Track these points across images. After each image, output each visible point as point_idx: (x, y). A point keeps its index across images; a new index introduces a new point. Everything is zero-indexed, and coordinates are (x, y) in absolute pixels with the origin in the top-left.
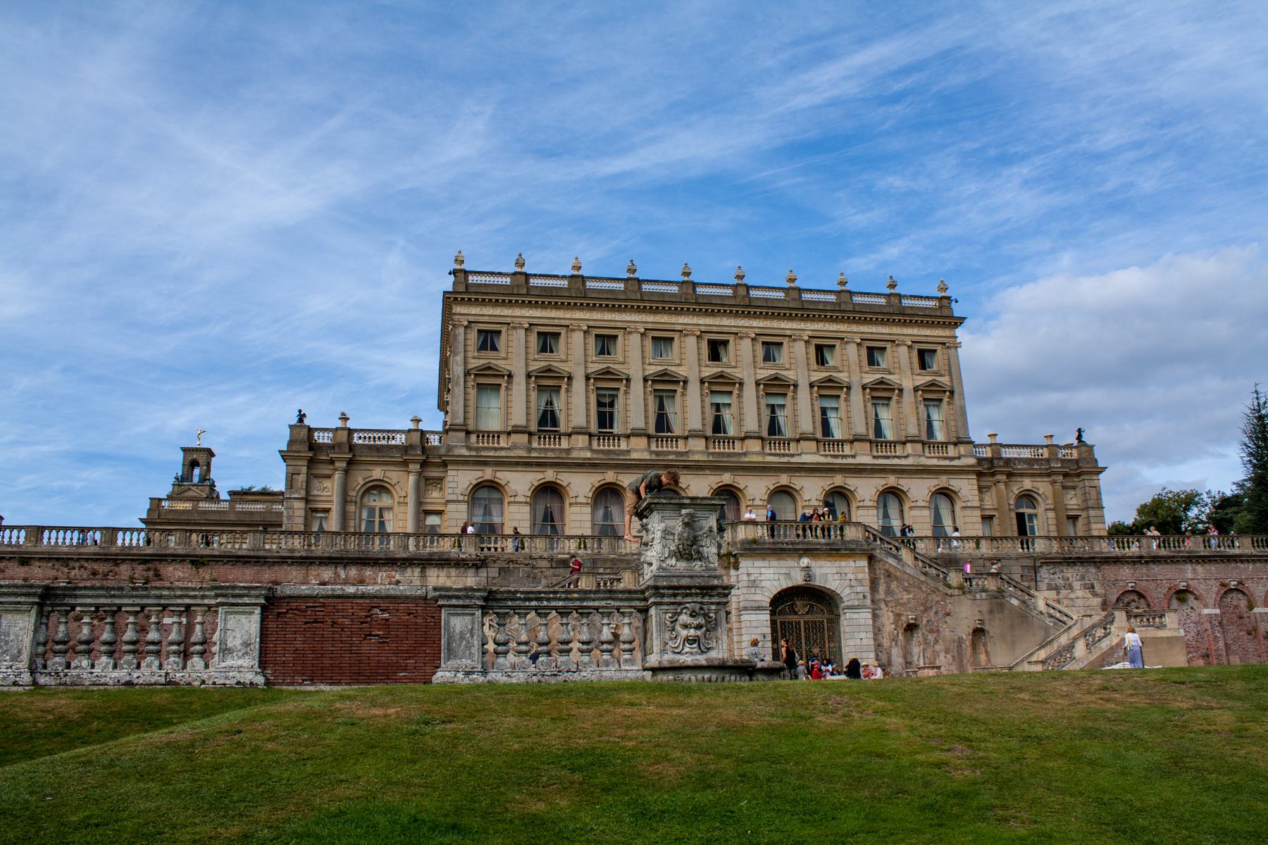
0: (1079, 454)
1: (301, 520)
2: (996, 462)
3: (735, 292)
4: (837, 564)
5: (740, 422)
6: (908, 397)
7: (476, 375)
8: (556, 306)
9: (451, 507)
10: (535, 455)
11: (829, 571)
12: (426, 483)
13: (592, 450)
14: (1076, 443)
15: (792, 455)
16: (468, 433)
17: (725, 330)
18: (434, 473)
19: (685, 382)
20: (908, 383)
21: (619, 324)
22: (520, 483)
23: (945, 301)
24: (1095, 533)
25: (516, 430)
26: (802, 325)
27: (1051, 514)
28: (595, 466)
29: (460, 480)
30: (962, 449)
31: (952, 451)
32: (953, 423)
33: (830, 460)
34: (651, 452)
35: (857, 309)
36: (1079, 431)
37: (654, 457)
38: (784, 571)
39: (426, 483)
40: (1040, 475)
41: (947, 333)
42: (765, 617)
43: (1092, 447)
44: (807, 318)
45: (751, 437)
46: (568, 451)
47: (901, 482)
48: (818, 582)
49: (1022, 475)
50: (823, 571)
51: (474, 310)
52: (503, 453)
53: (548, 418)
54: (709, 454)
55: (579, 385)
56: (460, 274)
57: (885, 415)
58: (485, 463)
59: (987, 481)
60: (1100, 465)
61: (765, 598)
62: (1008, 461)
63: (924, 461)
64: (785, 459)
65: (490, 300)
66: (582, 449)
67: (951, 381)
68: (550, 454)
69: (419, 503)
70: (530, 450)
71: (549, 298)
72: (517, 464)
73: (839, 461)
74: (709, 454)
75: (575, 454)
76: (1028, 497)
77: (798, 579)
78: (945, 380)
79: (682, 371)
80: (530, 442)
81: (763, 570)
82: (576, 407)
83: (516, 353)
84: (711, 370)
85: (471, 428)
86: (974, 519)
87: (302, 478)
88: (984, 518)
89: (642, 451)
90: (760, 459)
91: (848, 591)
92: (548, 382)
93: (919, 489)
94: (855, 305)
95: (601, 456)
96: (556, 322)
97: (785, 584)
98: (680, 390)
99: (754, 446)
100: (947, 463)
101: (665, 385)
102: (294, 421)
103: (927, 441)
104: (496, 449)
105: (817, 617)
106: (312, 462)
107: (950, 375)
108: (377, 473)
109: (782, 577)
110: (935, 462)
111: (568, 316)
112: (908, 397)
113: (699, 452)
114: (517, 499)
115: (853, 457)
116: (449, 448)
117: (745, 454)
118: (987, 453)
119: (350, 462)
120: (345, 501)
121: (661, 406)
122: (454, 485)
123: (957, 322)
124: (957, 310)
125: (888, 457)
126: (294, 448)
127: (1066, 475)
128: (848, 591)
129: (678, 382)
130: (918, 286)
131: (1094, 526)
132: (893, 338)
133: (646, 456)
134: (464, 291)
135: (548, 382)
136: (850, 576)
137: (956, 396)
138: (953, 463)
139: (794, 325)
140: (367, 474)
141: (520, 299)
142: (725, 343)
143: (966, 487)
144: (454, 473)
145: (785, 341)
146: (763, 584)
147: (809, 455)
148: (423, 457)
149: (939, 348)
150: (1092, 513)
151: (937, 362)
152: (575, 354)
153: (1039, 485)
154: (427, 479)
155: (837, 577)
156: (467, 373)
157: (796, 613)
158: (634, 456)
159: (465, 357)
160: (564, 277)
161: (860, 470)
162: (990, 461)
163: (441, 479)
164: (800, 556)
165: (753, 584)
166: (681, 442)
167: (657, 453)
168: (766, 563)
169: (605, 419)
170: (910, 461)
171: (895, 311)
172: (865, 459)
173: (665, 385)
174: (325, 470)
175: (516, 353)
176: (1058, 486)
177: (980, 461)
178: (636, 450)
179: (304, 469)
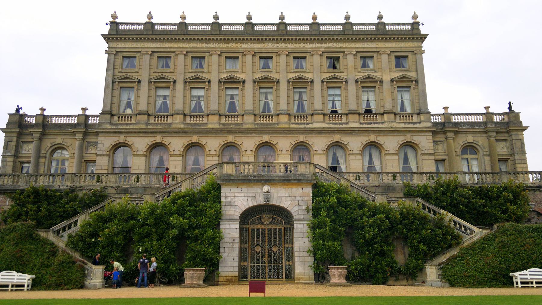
0: (509, 118)
1: (11, 168)
2: (447, 125)
3: (278, 28)
4: (290, 190)
5: (277, 104)
6: (386, 86)
7: (119, 82)
8: (168, 40)
9: (98, 159)
10: (151, 127)
11: (283, 195)
12: (85, 145)
13: (184, 123)
14: (508, 111)
15: (307, 124)
17: (270, 50)
19: (244, 82)
20: (386, 78)
21: (206, 50)
23: (415, 25)
24: (519, 170)
25: (141, 113)
26: (319, 45)
27: (487, 158)
28: (186, 132)
29: (106, 142)
30: (422, 117)
31: (415, 118)
32: (417, 101)
34: (220, 124)
35: (356, 33)
36: (510, 103)
37: (221, 126)
38: (251, 195)
39: (85, 145)
40: (479, 132)
41: (416, 44)
42: (236, 226)
43: (518, 114)
44: (322, 41)
45: (282, 114)
46: (170, 124)
47: (379, 138)
48: (274, 202)
49: (466, 133)
50: (280, 195)
51: (121, 45)
52: (131, 126)
54: (255, 124)
56: (114, 25)
58: (120, 133)
59: (440, 137)
60: (524, 125)
62: (457, 124)
63: (395, 125)
64: (303, 126)
65: (129, 39)
66: (179, 123)
67: (417, 75)
68: (159, 126)
69: (81, 156)
72: (139, 132)
73: (338, 126)
74: (255, 124)
75: (174, 126)
77: (260, 200)
78: (413, 75)
79: (242, 76)
80: (148, 119)
81: (237, 194)
85: (114, 113)
86: (430, 162)
87: (13, 144)
88: (436, 161)
89: (214, 123)
90: (287, 126)
91: (296, 208)
93: (391, 143)
94: (353, 31)
95: (190, 127)
96: (168, 50)
98: (241, 87)
99: (284, 119)
100: (411, 126)
102: (13, 111)
103: (402, 114)
104: (127, 124)
107: (417, 71)
108: (59, 140)
109: (249, 199)
110: (403, 125)
111: (176, 46)
112: (386, 86)
113: (250, 123)
114: (138, 153)
115: (347, 123)
117: (277, 124)
118: (439, 119)
119: (43, 134)
120: (38, 155)
122: (101, 146)
123: (423, 38)
124: (423, 30)
125: (370, 123)
126: (10, 127)
127: (498, 132)
128: (296, 208)
129: (239, 82)
130: (397, 16)
131: (518, 166)
132: (378, 50)
133: (217, 126)
134: (116, 34)
136: (298, 198)
137: (420, 82)
138: (416, 126)
139: (314, 45)
140: (52, 141)
141: (146, 37)
143: (425, 142)
144: (102, 138)
145: (308, 56)
146: (236, 204)
149: (410, 55)
150: (517, 157)
151: (409, 63)
153: (479, 139)
154: (88, 143)
155: (289, 199)
157: (262, 223)
158: (210, 126)
159: (114, 72)
160: (175, 24)
161: (351, 132)
162: (443, 124)
163: (96, 143)
164: (263, 184)
166: (240, 118)
167: (224, 124)
168: (239, 190)
170: (385, 125)
171: (381, 32)
172: (354, 124)
174: (29, 139)
175: (144, 69)
176: (492, 140)
177: (436, 124)
178: (211, 123)
179: (15, 139)
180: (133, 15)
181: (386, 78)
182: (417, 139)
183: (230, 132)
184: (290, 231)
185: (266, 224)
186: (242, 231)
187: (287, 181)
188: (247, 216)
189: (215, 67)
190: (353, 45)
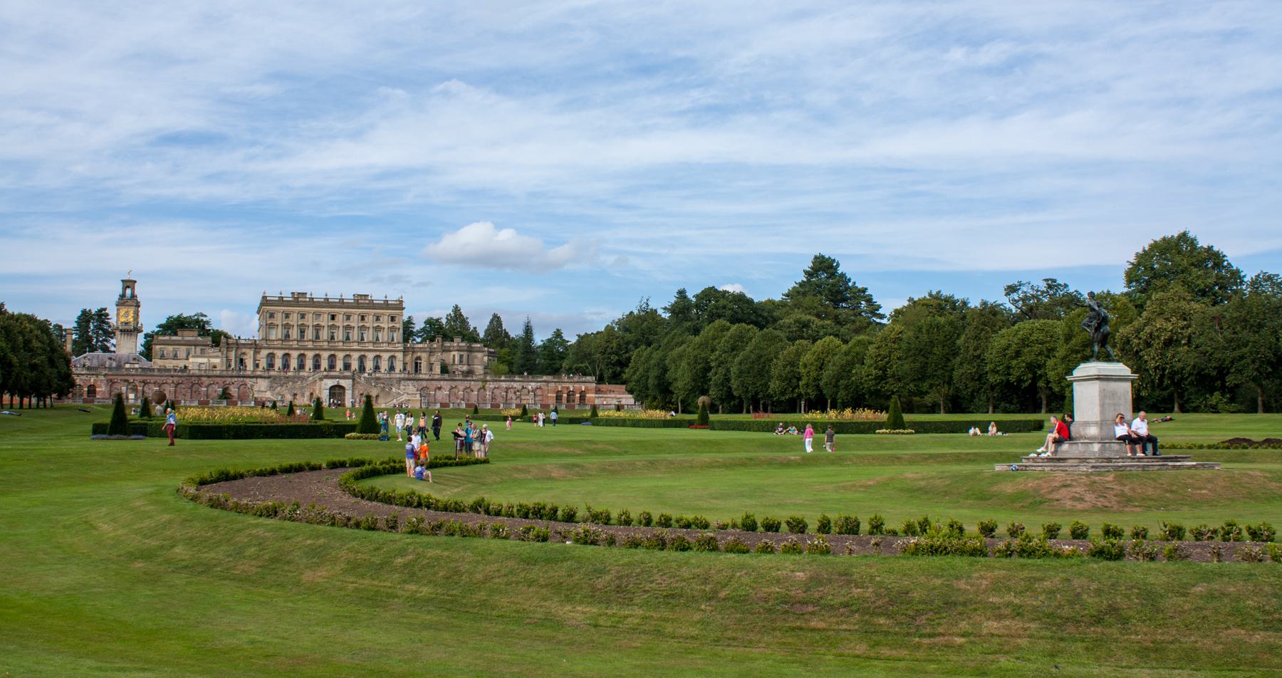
12: (256, 353)
22: (279, 353)
29: (264, 353)
39: (256, 353)
53: (287, 336)
56: (264, 298)
57: (380, 335)
71: (288, 304)
76: (419, 358)
82: (294, 333)
92: (287, 327)
101: (318, 328)
130: (393, 298)
135: (287, 327)
147: (355, 346)
148: (256, 347)
152: (294, 320)
169: (302, 336)
171: (386, 305)
173: (318, 328)
175: (279, 319)
180: (273, 294)
187: (345, 378)
188: (332, 388)
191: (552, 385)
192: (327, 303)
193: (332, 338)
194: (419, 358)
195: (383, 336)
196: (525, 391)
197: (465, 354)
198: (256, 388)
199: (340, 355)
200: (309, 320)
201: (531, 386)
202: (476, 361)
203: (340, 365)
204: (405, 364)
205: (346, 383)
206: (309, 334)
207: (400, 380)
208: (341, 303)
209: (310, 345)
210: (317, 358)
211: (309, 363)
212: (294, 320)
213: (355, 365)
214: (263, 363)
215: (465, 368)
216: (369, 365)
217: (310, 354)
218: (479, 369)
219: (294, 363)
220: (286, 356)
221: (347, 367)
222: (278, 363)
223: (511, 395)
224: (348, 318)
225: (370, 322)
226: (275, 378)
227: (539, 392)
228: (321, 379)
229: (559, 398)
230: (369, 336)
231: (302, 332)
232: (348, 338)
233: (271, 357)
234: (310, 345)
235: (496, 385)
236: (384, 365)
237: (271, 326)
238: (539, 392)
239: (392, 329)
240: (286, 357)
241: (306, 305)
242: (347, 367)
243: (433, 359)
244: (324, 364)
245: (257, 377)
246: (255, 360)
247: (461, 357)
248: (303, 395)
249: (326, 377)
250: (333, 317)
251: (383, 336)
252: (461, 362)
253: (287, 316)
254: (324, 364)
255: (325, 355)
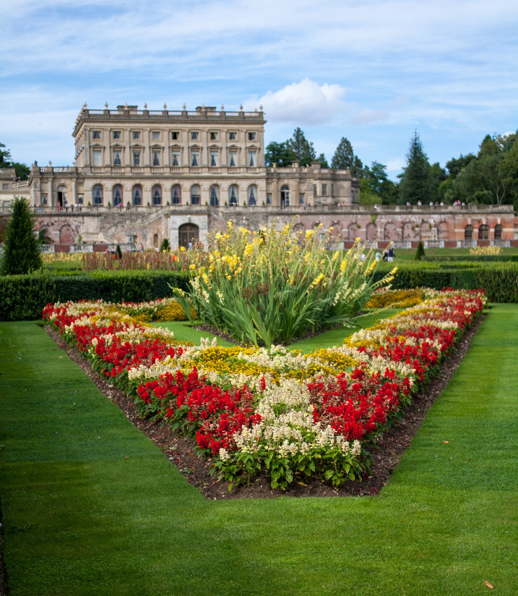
5: (182, 162)
6: (243, 151)
9: (86, 193)
12: (79, 184)
16: (91, 168)
18: (81, 181)
20: (243, 146)
22: (108, 184)
25: (107, 167)
29: (89, 184)
33: (212, 175)
34: (151, 173)
39: (79, 184)
40: (291, 178)
41: (260, 126)
46: (124, 173)
49: (284, 179)
51: (92, 124)
53: (117, 162)
55: (127, 150)
57: (235, 157)
61: (177, 226)
70: (112, 173)
71: (117, 119)
75: (126, 174)
76: (286, 187)
77: (187, 221)
78: (257, 145)
79: (162, 144)
82: (126, 158)
83: (105, 140)
84: (173, 143)
85: (92, 165)
97: (183, 222)
105: (193, 231)
106: (41, 179)
116: (85, 173)
121: (156, 156)
123: (264, 122)
129: (160, 148)
142: (178, 133)
147: (205, 173)
148: (77, 176)
156: (90, 147)
158: (146, 174)
165: (174, 223)
169: (137, 161)
170: (241, 175)
171: (242, 118)
172: (225, 174)
175: (105, 140)
179: (39, 181)
181: (243, 146)
182: (257, 182)
183: (157, 178)
184: (197, 233)
185: (188, 231)
186: (180, 233)
187: (197, 213)
189: (146, 139)
190: (225, 126)
191: (459, 217)
192: (166, 117)
193: (175, 163)
194: (286, 187)
195: (239, 159)
196: (426, 226)
197: (329, 183)
198: (82, 230)
199: (186, 185)
200: (145, 140)
201: (434, 219)
202: (342, 192)
203: (186, 198)
204: (269, 194)
205: (200, 220)
206: (146, 158)
207: (267, 215)
208: (185, 117)
209: (147, 172)
210: (157, 190)
211: (147, 197)
212: (125, 139)
213: (205, 198)
214: (88, 198)
215: (329, 200)
216: (224, 197)
217: (148, 185)
218: (346, 200)
219: (127, 197)
220: (118, 187)
221: (195, 200)
222: (108, 197)
223: (408, 231)
224: (194, 136)
225: (222, 140)
226: (106, 216)
227: (443, 227)
228: (167, 216)
229: (468, 235)
230: (221, 159)
231: (136, 157)
232: (194, 163)
233: (98, 188)
234: (147, 172)
235: (389, 218)
236: (242, 197)
237: (97, 148)
238: (443, 227)
239: (252, 150)
240: (117, 189)
241: (139, 120)
242: (195, 200)
243: (304, 188)
244: (166, 197)
245: (84, 215)
246: (77, 194)
247: (324, 186)
248: (145, 237)
249: (174, 213)
250: (175, 136)
251: (239, 159)
252: (324, 192)
253: (116, 135)
254: (166, 197)
255: (167, 185)
